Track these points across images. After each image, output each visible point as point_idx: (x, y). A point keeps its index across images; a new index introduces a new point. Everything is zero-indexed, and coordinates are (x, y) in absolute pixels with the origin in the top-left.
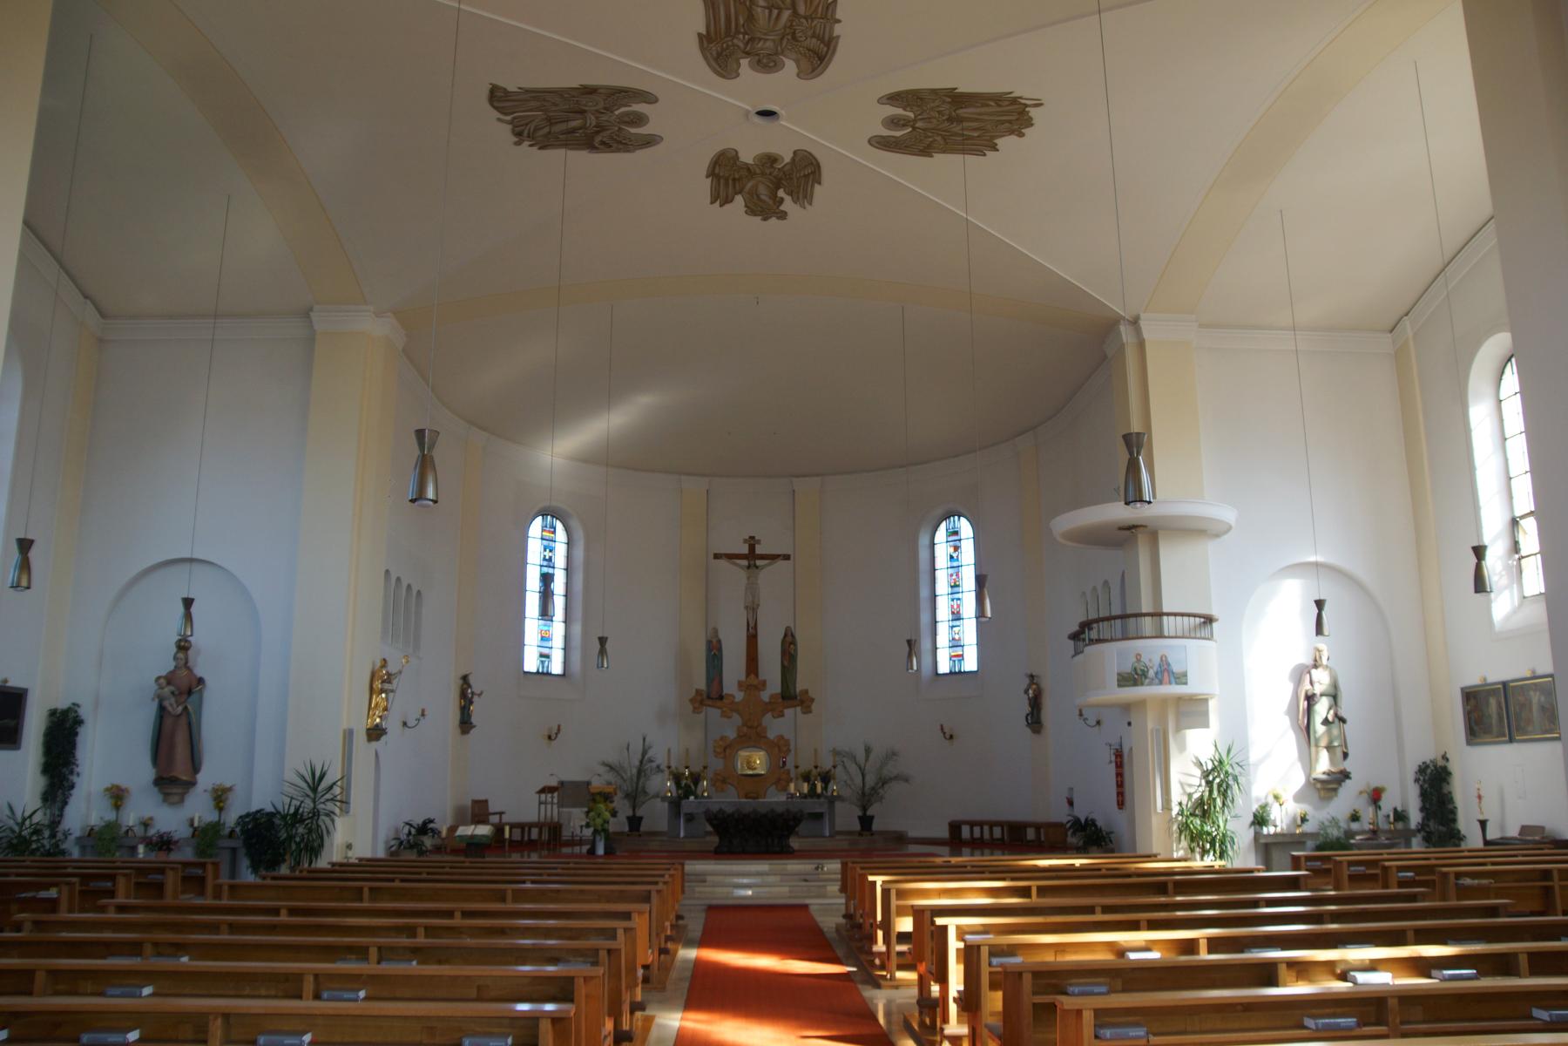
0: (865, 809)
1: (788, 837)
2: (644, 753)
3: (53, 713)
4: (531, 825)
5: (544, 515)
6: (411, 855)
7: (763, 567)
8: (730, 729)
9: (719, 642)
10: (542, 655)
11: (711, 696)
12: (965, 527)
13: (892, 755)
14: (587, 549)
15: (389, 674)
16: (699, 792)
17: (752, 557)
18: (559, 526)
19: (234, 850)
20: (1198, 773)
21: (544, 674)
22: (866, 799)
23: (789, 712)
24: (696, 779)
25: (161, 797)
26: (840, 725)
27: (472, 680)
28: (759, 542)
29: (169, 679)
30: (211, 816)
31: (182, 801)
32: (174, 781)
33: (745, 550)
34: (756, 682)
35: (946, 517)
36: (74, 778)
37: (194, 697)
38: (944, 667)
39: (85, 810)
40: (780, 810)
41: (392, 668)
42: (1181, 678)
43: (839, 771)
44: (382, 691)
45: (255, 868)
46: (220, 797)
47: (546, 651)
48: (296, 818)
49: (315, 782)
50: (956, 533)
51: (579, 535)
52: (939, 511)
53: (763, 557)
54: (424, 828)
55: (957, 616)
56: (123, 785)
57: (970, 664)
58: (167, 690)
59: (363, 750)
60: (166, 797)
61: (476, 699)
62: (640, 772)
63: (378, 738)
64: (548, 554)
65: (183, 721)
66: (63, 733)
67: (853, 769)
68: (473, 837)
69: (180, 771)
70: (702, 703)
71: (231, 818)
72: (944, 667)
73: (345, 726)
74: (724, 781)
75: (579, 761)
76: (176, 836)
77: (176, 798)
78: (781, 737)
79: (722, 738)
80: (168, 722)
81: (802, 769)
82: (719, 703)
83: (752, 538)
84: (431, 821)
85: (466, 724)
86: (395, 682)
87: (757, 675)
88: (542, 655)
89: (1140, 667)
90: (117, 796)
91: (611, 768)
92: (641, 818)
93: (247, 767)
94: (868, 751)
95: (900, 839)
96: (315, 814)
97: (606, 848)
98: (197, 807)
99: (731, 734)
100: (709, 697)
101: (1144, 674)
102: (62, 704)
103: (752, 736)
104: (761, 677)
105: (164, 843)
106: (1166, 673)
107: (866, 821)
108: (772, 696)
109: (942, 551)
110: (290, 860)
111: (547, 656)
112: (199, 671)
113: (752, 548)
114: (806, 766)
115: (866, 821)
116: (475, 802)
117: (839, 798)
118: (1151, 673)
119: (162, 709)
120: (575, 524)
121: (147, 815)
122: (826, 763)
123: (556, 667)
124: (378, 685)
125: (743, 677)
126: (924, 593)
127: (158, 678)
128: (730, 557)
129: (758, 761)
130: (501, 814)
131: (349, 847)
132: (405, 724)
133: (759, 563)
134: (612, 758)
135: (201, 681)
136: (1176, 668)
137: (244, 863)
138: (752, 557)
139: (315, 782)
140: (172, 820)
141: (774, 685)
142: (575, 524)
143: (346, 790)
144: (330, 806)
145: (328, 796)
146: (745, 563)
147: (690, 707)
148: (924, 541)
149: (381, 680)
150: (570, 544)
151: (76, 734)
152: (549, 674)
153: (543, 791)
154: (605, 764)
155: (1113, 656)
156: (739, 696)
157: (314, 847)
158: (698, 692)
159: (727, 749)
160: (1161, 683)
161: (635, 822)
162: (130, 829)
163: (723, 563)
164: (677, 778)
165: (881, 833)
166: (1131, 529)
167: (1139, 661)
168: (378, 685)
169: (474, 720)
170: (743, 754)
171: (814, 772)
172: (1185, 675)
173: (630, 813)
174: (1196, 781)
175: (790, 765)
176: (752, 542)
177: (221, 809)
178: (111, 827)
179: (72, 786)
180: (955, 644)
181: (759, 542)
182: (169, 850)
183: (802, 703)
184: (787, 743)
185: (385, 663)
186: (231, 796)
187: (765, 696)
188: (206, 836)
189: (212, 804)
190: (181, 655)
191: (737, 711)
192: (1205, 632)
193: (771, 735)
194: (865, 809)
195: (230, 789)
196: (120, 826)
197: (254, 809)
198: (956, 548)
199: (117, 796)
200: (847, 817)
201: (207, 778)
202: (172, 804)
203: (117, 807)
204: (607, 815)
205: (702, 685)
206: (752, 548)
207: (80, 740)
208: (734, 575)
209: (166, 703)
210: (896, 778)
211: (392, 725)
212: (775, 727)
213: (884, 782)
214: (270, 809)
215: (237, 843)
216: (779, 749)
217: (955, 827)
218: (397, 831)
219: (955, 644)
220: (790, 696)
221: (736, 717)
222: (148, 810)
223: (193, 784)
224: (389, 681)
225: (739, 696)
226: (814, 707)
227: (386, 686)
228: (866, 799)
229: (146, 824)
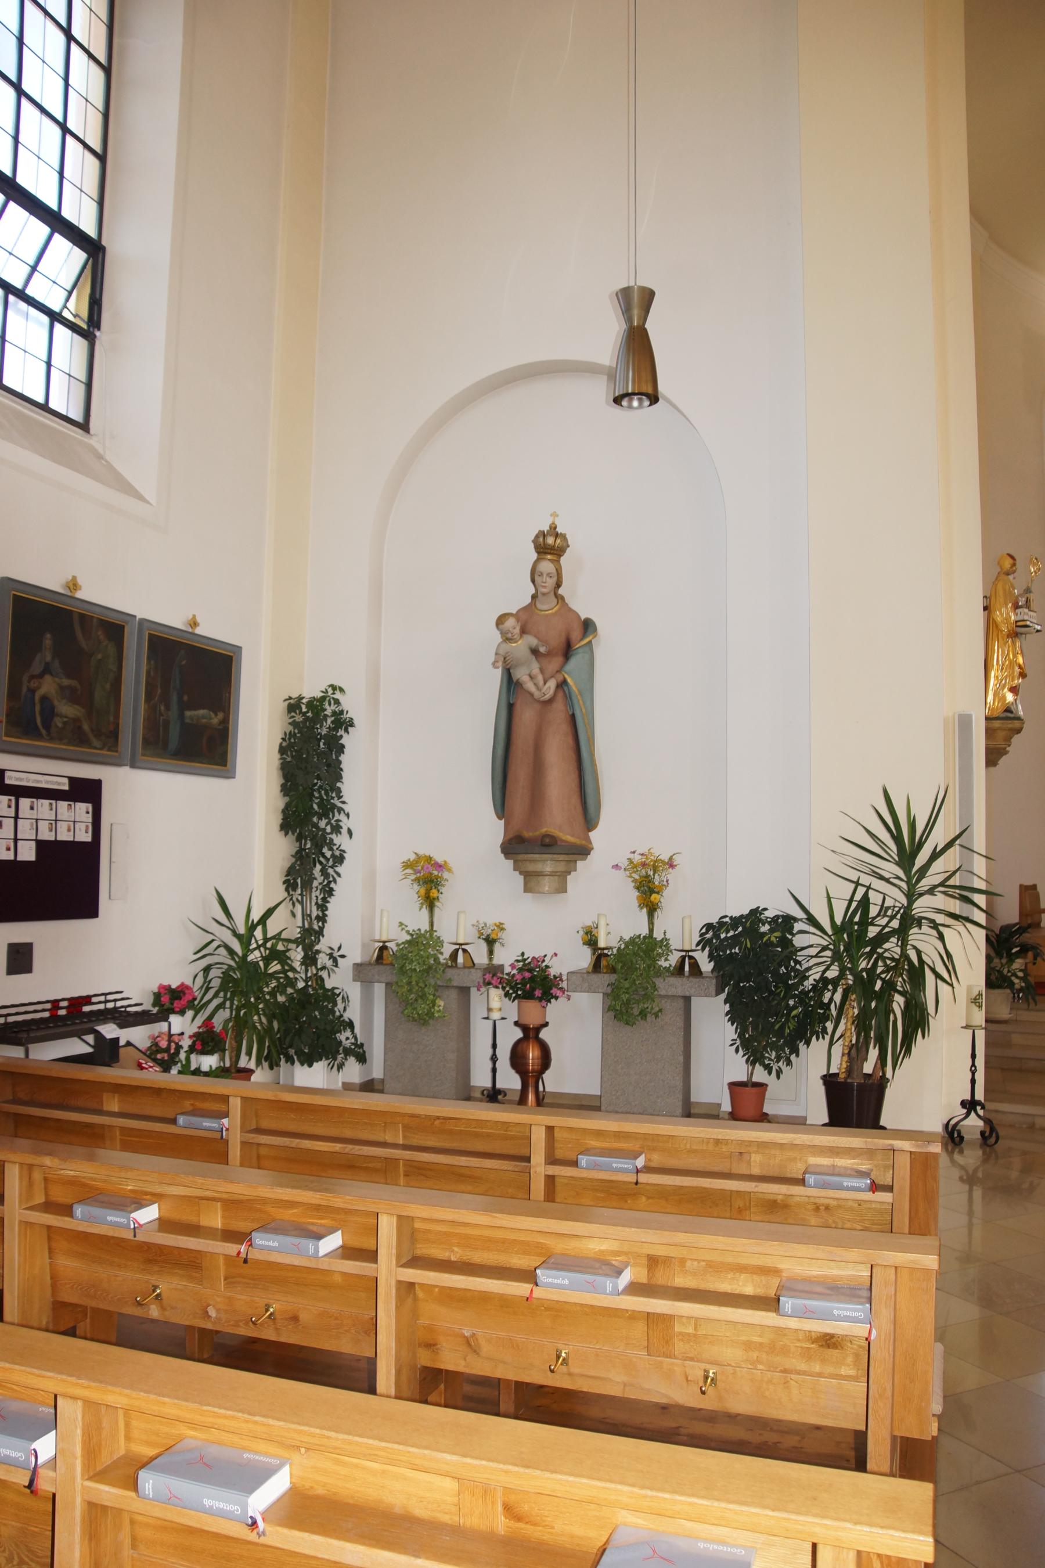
3: (293, 706)
29: (526, 620)
30: (635, 924)
31: (562, 889)
32: (548, 844)
36: (341, 840)
39: (369, 908)
58: (521, 647)
60: (531, 881)
65: (558, 713)
66: (314, 748)
69: (557, 819)
71: (681, 925)
80: (526, 716)
98: (597, 903)
102: (311, 690)
105: (534, 984)
119: (511, 684)
121: (491, 919)
127: (501, 620)
135: (588, 626)
162: (461, 947)
177: (652, 909)
178: (421, 943)
182: (547, 996)
190: (547, 566)
196: (439, 942)
199: (429, 879)
201: (613, 840)
203: (430, 903)
207: (347, 760)
209: (521, 674)
214: (777, 905)
222: (495, 909)
223: (583, 851)
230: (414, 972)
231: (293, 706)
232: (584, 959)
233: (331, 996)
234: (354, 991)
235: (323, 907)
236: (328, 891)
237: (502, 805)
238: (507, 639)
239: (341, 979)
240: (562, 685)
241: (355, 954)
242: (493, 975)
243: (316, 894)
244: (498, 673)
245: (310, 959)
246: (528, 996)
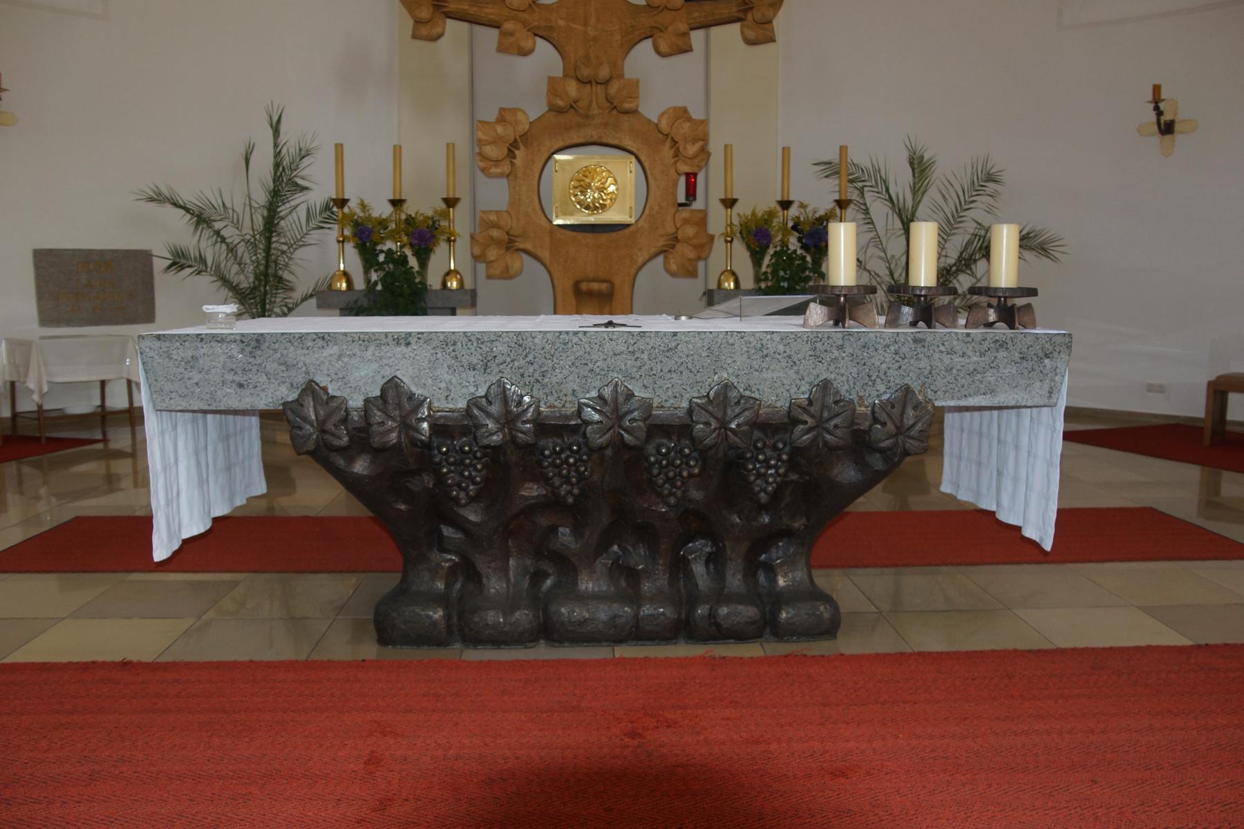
16: (434, 281)
24: (424, 237)
74: (510, 244)
78: (682, 114)
79: (504, 116)
81: (743, 209)
94: (919, 167)
99: (535, 109)
114: (757, 199)
159: (513, 149)
164: (365, 235)
193: (652, 107)
216: (677, 151)
221: (543, 47)
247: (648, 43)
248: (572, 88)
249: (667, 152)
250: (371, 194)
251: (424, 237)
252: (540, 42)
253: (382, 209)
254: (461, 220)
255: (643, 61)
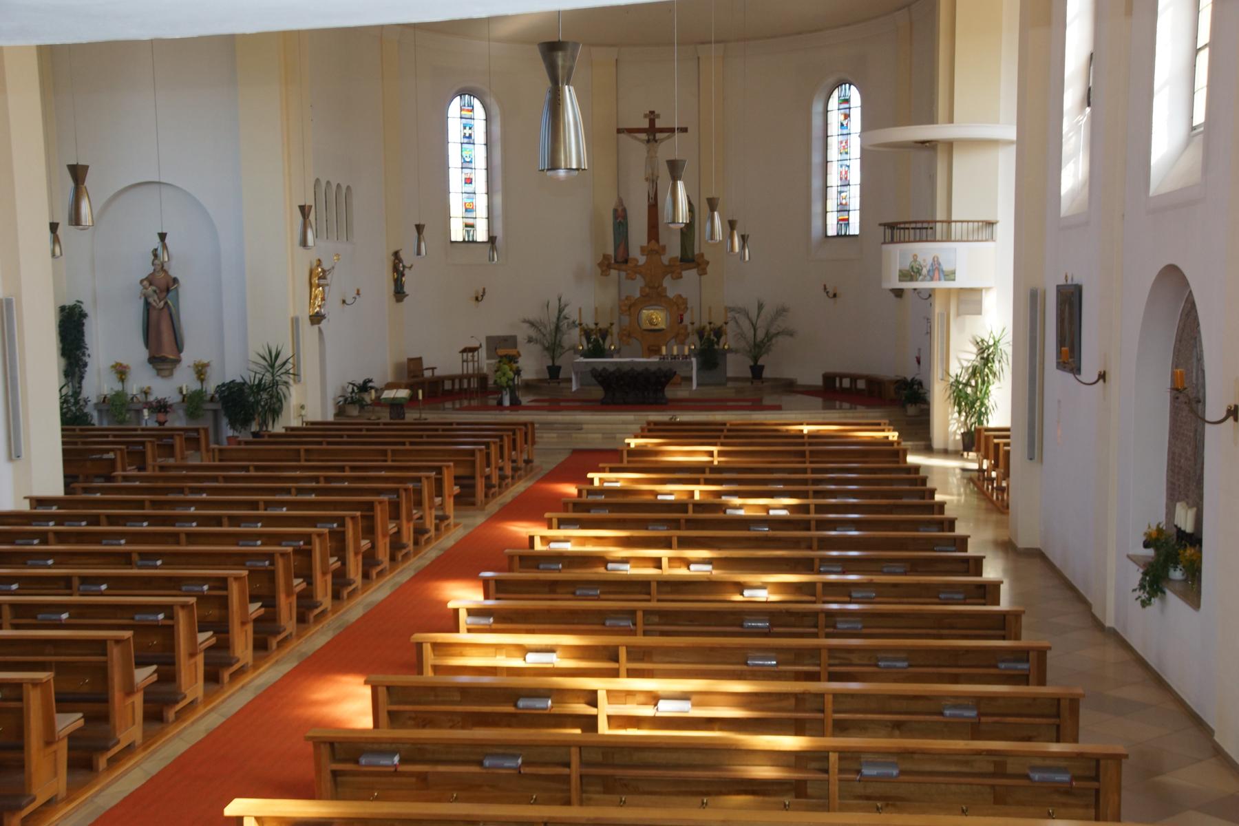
0: (756, 359)
1: (662, 390)
2: (560, 311)
3: (62, 309)
4: (461, 378)
5: (461, 94)
6: (354, 411)
7: (662, 140)
8: (635, 288)
9: (624, 210)
10: (467, 226)
11: (617, 261)
12: (855, 95)
13: (781, 311)
14: (503, 126)
15: (323, 271)
16: (607, 346)
17: (652, 131)
18: (476, 103)
19: (215, 412)
20: (975, 350)
21: (469, 243)
22: (758, 348)
23: (684, 273)
24: (604, 334)
25: (154, 372)
26: (736, 284)
27: (402, 255)
28: (658, 116)
29: (150, 280)
30: (195, 386)
31: (171, 374)
32: (164, 360)
33: (645, 124)
34: (656, 247)
35: (839, 84)
36: (86, 359)
37: (171, 294)
38: (832, 231)
40: (653, 368)
41: (326, 266)
42: (950, 276)
43: (730, 329)
44: (319, 286)
45: (233, 425)
46: (201, 371)
47: (470, 221)
48: (260, 387)
49: (272, 360)
50: (847, 101)
51: (495, 111)
52: (831, 80)
53: (662, 130)
54: (364, 387)
55: (846, 184)
56: (125, 363)
57: (854, 229)
59: (309, 333)
60: (159, 372)
61: (407, 272)
62: (557, 328)
63: (319, 322)
64: (468, 132)
67: (745, 324)
68: (394, 399)
69: (168, 353)
70: (609, 267)
71: (211, 387)
72: (832, 231)
73: (292, 314)
74: (629, 336)
75: (498, 320)
76: (170, 401)
77: (167, 373)
79: (627, 298)
80: (154, 314)
82: (624, 267)
83: (652, 112)
84: (370, 381)
85: (399, 294)
86: (329, 277)
87: (657, 241)
88: (467, 226)
89: (916, 265)
90: (121, 372)
91: (532, 324)
92: (559, 368)
93: (220, 349)
94: (760, 307)
95: (789, 386)
96: (275, 384)
97: (511, 400)
98: (184, 379)
99: (638, 295)
100: (616, 262)
101: (919, 272)
102: (69, 302)
103: (654, 296)
104: (662, 242)
105: (161, 407)
106: (937, 270)
107: (757, 371)
108: (671, 260)
109: (835, 118)
110: (258, 419)
111: (472, 226)
112: (173, 273)
113: (652, 122)
115: (757, 371)
116: (410, 360)
117: (730, 350)
118: (925, 271)
119: (147, 304)
120: (491, 101)
121: (145, 385)
122: (718, 322)
123: (481, 235)
124: (315, 281)
125: (644, 242)
126: (816, 159)
127: (142, 282)
128: (631, 131)
129: (657, 317)
130: (433, 369)
131: (302, 407)
132: (344, 302)
133: (659, 136)
134: (533, 315)
135: (175, 280)
136: (946, 267)
137: (224, 421)
138: (652, 131)
139: (272, 360)
140: (165, 389)
141: (674, 250)
142: (491, 101)
143: (297, 365)
144: (284, 378)
145: (283, 370)
146: (644, 136)
147: (599, 271)
148: (817, 108)
149: (318, 276)
150: (488, 120)
151: (83, 324)
152: (474, 242)
153: (464, 351)
154: (525, 321)
155: (900, 255)
156: (642, 260)
157: (275, 410)
158: (606, 257)
159: (631, 307)
160: (932, 279)
161: (554, 371)
163: (623, 136)
164: (587, 333)
165: (768, 380)
166: (928, 145)
167: (915, 260)
168: (315, 281)
169: (406, 289)
170: (645, 312)
171: (708, 328)
172: (954, 273)
173: (550, 364)
174: (973, 357)
175: (687, 320)
176: (652, 116)
177: (202, 381)
178: (119, 395)
179: (85, 365)
180: (843, 209)
181: (658, 116)
182: (166, 412)
183: (698, 265)
184: (685, 302)
185: (319, 262)
186: (208, 370)
187: (665, 259)
188: (193, 402)
189: (195, 376)
191: (640, 273)
192: (985, 233)
193: (671, 294)
194: (756, 359)
195: (207, 365)
197: (228, 380)
198: (847, 116)
199: (121, 372)
200: (736, 366)
201: (189, 357)
202: (163, 377)
203: (122, 380)
204: (511, 374)
205: (610, 251)
206: (652, 122)
207: (86, 329)
208: (636, 148)
209: (151, 300)
210: (778, 333)
211: (332, 310)
212: (672, 288)
213: (769, 337)
214: (239, 380)
215: (218, 406)
216: (678, 307)
217: (829, 379)
218: (344, 389)
219: (843, 209)
220: (690, 259)
223: (178, 361)
224: (324, 277)
225: (642, 260)
226: (709, 269)
227: (322, 282)
228: (758, 348)
229: (146, 393)
230: (115, 405)
231: (62, 309)
232: (178, 398)
233: (86, 415)
234: (95, 414)
235: (80, 383)
236: (82, 378)
237: (147, 344)
238: (145, 288)
239: (89, 409)
240: (166, 303)
241: (94, 400)
242: (148, 405)
243: (76, 379)
244: (142, 301)
245: (77, 402)
246: (160, 411)
247: (669, 276)
248: (647, 290)
249: (675, 308)
250: (589, 322)
251: (604, 334)
252: (638, 276)
253: (592, 326)
254: (615, 329)
255: (667, 282)
